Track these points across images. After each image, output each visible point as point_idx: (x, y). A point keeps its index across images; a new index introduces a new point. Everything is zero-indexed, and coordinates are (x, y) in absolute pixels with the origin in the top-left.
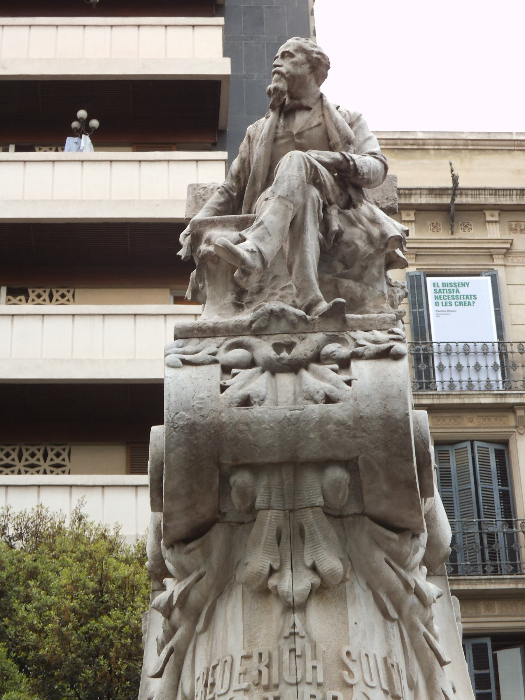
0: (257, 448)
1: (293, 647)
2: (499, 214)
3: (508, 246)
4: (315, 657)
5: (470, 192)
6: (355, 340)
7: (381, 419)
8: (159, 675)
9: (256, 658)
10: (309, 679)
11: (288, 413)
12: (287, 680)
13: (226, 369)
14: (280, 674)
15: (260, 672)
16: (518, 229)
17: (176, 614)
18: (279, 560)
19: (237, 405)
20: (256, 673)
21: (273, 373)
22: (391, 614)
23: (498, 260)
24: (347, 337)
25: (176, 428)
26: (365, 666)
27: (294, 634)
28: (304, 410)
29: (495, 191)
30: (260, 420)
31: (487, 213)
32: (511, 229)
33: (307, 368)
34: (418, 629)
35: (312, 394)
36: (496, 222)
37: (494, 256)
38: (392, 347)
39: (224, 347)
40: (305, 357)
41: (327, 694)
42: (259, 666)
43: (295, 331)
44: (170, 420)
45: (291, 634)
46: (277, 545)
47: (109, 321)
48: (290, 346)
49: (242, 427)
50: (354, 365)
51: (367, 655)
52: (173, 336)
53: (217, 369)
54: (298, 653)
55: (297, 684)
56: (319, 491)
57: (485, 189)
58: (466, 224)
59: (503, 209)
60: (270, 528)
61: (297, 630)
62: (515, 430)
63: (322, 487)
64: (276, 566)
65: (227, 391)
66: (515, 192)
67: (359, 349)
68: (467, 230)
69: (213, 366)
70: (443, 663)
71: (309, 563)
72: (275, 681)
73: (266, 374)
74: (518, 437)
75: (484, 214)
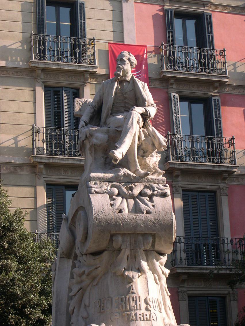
17: (84, 277)
71: (137, 268)
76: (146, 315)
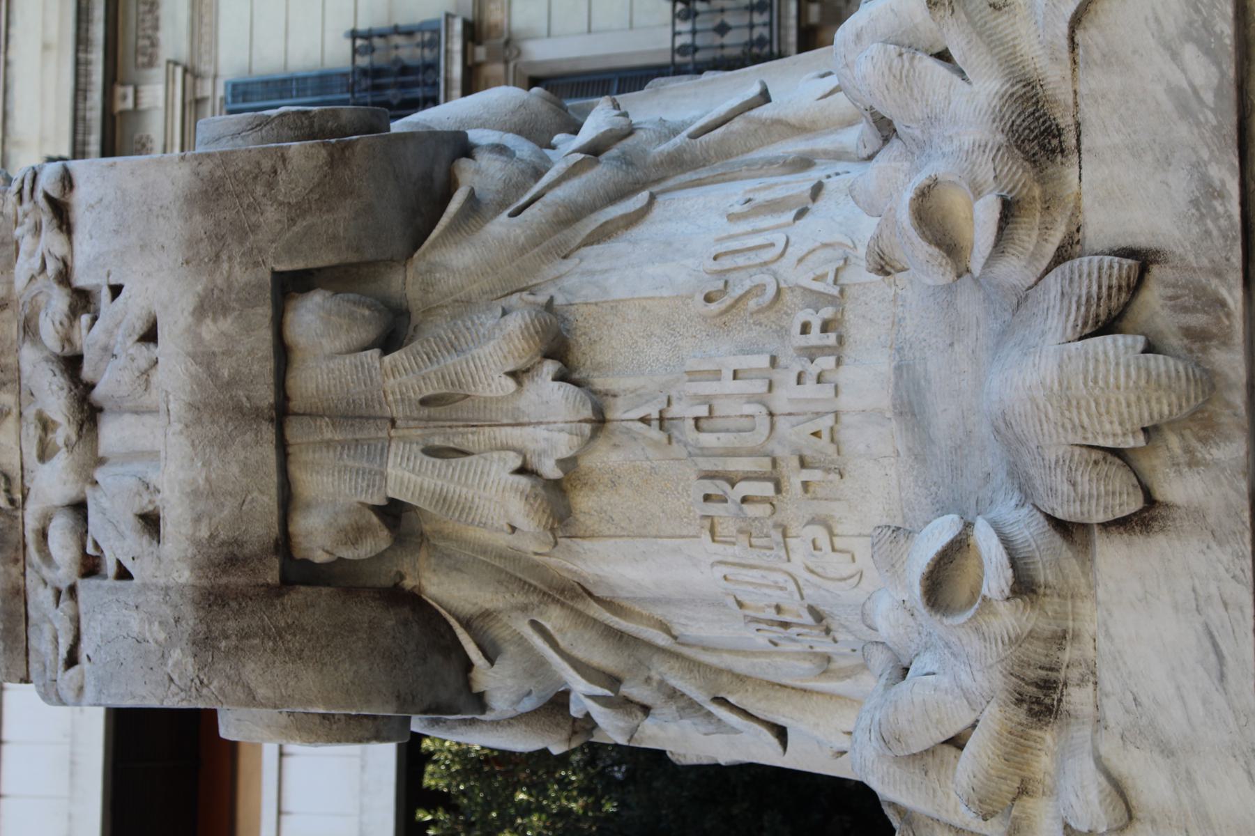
0: (250, 497)
1: (692, 422)
2: (124, 84)
3: (179, 71)
4: (716, 375)
5: (80, 137)
6: (32, 278)
7: (191, 218)
8: (781, 733)
9: (714, 509)
10: (760, 387)
11: (178, 427)
12: (764, 438)
13: (90, 567)
14: (752, 453)
15: (745, 500)
16: (150, 50)
17: (633, 690)
18: (503, 454)
19: (155, 542)
20: (750, 510)
21: (101, 462)
22: (638, 206)
23: (206, 89)
24: (27, 298)
25: (201, 682)
26: (741, 261)
27: (661, 419)
28: (169, 390)
29: (80, 92)
30: (188, 490)
31: (120, 106)
32: (151, 64)
33: (91, 387)
34: (680, 151)
35: (137, 374)
36: (136, 92)
37: (199, 95)
38: (48, 197)
39: (45, 572)
40: (66, 390)
41: (797, 345)
42: (734, 501)
43: (15, 411)
44: (183, 694)
45: (661, 428)
46: (467, 460)
47: (289, 804)
48: (46, 425)
49: (204, 533)
50: (81, 279)
51: (715, 258)
52: (24, 685)
53: (87, 588)
54: (703, 411)
55: (771, 414)
56: (349, 360)
57: (75, 109)
58: (139, 147)
59: (112, 78)
60: (429, 472)
61: (655, 415)
62: (511, 65)
63: (340, 353)
64: (517, 463)
65: (128, 564)
66: (82, 55)
67: (52, 267)
68: (149, 145)
69: (82, 594)
70: (765, 97)
71: (510, 384)
72: (764, 465)
73: (98, 475)
74: (524, 59)
75: (123, 113)
76: (805, 328)
